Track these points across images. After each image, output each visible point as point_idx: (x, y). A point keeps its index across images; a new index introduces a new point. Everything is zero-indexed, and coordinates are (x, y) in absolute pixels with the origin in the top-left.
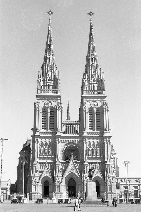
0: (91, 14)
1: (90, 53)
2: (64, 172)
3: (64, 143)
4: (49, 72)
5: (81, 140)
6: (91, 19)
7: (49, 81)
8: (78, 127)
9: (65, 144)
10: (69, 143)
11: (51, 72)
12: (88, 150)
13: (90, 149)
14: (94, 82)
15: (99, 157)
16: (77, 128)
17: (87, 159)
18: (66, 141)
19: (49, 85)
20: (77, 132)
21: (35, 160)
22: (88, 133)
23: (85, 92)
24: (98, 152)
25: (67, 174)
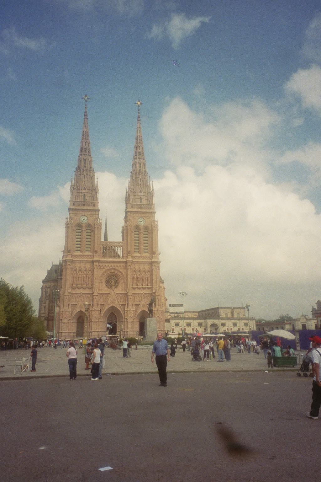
1: (136, 155)
3: (103, 269)
4: (85, 178)
5: (124, 265)
6: (139, 110)
8: (120, 249)
9: (104, 270)
11: (87, 178)
12: (133, 278)
13: (135, 277)
16: (119, 251)
17: (131, 288)
18: (105, 266)
20: (119, 256)
21: (67, 290)
23: (129, 206)
24: (145, 281)
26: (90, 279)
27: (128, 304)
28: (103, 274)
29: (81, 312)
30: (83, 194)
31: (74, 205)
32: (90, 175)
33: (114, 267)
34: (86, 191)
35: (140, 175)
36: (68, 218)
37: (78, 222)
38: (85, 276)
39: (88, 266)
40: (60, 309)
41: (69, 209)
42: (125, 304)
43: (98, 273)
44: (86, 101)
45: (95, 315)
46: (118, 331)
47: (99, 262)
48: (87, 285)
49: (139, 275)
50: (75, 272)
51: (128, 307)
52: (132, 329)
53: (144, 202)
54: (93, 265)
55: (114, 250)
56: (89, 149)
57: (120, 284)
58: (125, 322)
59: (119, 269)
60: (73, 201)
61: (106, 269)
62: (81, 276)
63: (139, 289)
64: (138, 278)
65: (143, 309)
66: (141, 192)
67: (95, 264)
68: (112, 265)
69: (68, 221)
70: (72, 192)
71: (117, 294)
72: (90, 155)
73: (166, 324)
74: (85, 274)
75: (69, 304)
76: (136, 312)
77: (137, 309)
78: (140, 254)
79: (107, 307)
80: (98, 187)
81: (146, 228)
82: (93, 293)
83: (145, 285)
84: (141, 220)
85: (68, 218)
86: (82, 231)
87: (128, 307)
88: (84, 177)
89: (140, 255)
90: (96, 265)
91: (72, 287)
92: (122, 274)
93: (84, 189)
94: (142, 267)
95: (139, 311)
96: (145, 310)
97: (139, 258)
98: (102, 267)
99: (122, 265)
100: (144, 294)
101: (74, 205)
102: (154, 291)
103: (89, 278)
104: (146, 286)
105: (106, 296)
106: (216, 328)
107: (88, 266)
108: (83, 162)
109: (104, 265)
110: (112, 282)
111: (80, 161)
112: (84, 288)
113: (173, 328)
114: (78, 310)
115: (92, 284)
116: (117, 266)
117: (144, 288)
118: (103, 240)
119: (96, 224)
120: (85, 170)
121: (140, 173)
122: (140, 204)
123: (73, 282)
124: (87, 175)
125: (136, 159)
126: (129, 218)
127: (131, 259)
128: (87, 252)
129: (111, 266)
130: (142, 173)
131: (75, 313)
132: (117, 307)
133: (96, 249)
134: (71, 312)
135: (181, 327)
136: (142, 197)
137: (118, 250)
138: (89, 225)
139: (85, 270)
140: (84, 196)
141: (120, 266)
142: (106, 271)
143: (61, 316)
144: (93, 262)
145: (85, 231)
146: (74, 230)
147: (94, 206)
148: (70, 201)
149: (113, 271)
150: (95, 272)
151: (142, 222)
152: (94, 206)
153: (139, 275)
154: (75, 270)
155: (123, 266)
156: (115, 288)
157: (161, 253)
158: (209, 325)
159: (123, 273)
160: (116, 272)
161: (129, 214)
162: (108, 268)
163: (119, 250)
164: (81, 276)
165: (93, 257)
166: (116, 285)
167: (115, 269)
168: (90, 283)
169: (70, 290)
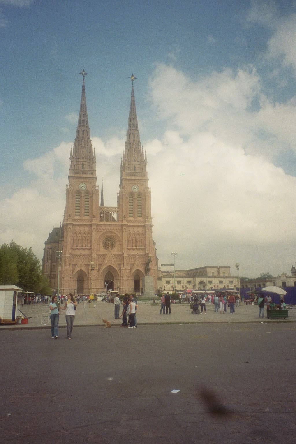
1: (130, 127)
3: (101, 231)
4: (83, 148)
7: (84, 159)
8: (116, 214)
9: (102, 233)
10: (107, 232)
11: (85, 148)
13: (130, 239)
14: (135, 163)
15: (139, 248)
16: (115, 215)
17: (126, 250)
19: (83, 163)
20: (116, 221)
21: (68, 251)
22: (127, 221)
26: (88, 241)
27: (123, 264)
29: (81, 271)
30: (82, 163)
31: (73, 173)
32: (88, 145)
33: (110, 230)
34: (85, 160)
35: (134, 145)
36: (68, 185)
38: (84, 238)
39: (87, 229)
40: (62, 268)
41: (69, 177)
42: (121, 264)
43: (95, 236)
44: (84, 76)
45: (94, 274)
46: (114, 288)
47: (97, 225)
48: (86, 247)
49: (134, 237)
50: (75, 235)
51: (123, 267)
52: (127, 286)
53: (138, 170)
54: (92, 229)
55: (111, 215)
56: (87, 121)
57: (116, 245)
58: (121, 279)
59: (115, 232)
60: (73, 170)
61: (103, 232)
62: (80, 238)
63: (134, 250)
64: (132, 240)
65: (137, 269)
66: (135, 161)
67: (93, 227)
68: (109, 228)
69: (68, 188)
70: (72, 161)
71: (113, 254)
72: (87, 127)
73: (158, 282)
74: (84, 236)
75: (70, 264)
76: (131, 271)
77: (131, 269)
78: (134, 218)
79: (104, 267)
80: (95, 156)
81: (140, 194)
82: (92, 254)
83: (138, 247)
84: (135, 187)
85: (68, 185)
86: (81, 197)
87: (123, 267)
88: (82, 146)
89: (134, 219)
90: (94, 228)
91: (72, 248)
94: (136, 230)
95: (134, 270)
96: (139, 269)
97: (134, 222)
98: (100, 231)
99: (118, 228)
100: (138, 255)
101: (73, 173)
102: (147, 252)
103: (88, 240)
104: (140, 248)
105: (104, 257)
106: (204, 285)
107: (87, 229)
108: (81, 133)
109: (101, 229)
110: (109, 244)
111: (78, 132)
112: (84, 249)
113: (164, 285)
114: (78, 269)
116: (113, 229)
117: (138, 250)
118: (100, 205)
119: (94, 191)
120: (83, 140)
121: (134, 144)
122: (134, 173)
123: (74, 244)
124: (85, 145)
125: (130, 130)
126: (124, 185)
127: (126, 223)
128: (85, 216)
129: (108, 229)
130: (135, 144)
131: (76, 271)
132: (114, 267)
133: (94, 214)
134: (72, 271)
135: (172, 285)
136: (136, 165)
137: (114, 214)
138: (87, 192)
139: (84, 233)
140: (83, 165)
141: (116, 229)
142: (103, 234)
143: (63, 274)
144: (91, 226)
145: (83, 197)
146: (74, 196)
147: (92, 173)
148: (70, 169)
149: (109, 234)
150: (94, 234)
151: (135, 188)
152: (92, 173)
153: (134, 237)
154: (75, 233)
155: (119, 229)
156: (112, 249)
157: (153, 217)
158: (197, 283)
160: (112, 234)
161: (124, 181)
162: (105, 231)
163: (115, 214)
164: (80, 238)
165: (92, 221)
166: (113, 246)
167: (111, 232)
168: (89, 245)
169: (70, 251)
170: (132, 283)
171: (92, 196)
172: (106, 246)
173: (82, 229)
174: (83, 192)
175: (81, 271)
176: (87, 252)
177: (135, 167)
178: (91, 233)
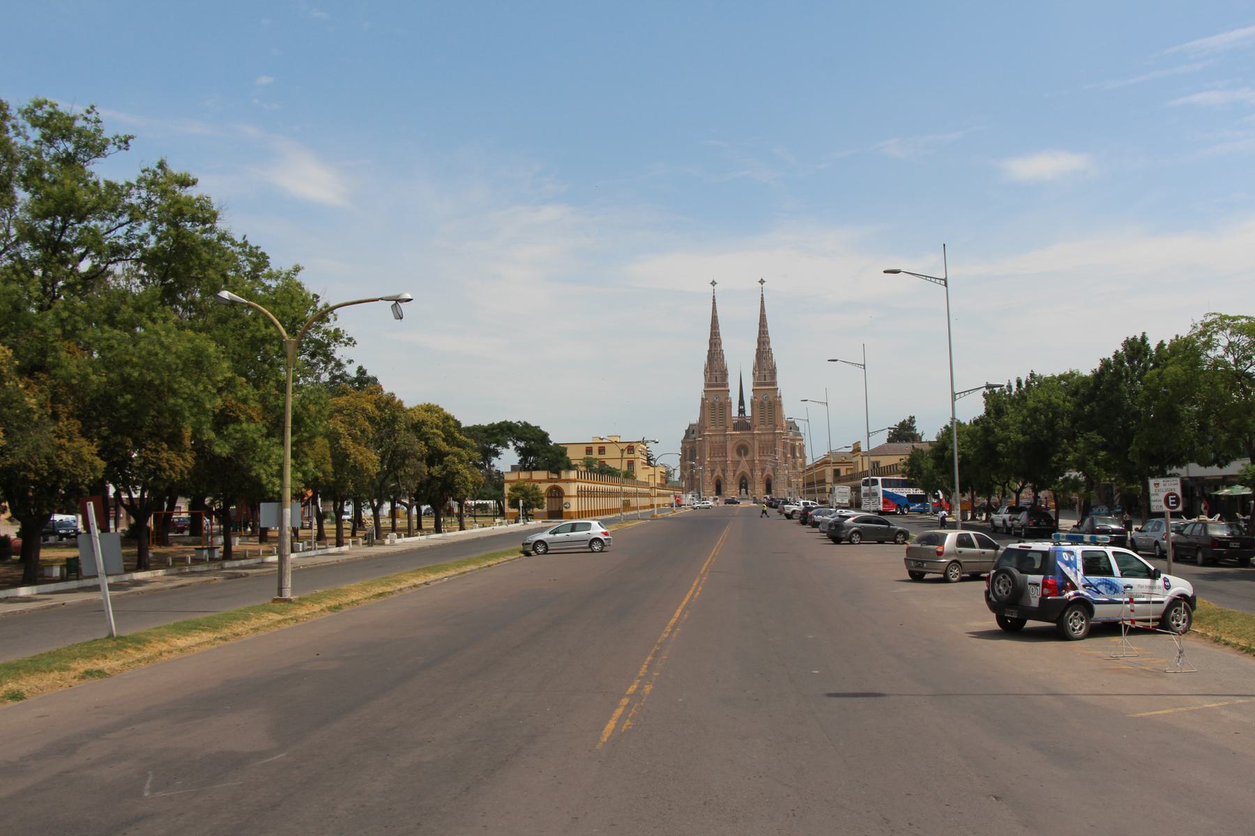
0: (762, 282)
2: (735, 471)
12: (760, 447)
25: (738, 473)
28: (735, 444)
29: (718, 476)
37: (711, 401)
39: (722, 438)
41: (705, 391)
43: (730, 445)
59: (748, 440)
61: (736, 440)
76: (762, 475)
82: (726, 461)
92: (750, 444)
93: (716, 371)
94: (767, 437)
115: (726, 453)
138: (721, 404)
142: (737, 442)
150: (728, 443)
159: (751, 443)
160: (745, 443)
166: (746, 454)
167: (745, 441)
170: (764, 486)
171: (725, 408)
172: (739, 453)
173: (718, 438)
174: (717, 404)
175: (718, 476)
176: (723, 459)
177: (765, 376)
178: (725, 442)
